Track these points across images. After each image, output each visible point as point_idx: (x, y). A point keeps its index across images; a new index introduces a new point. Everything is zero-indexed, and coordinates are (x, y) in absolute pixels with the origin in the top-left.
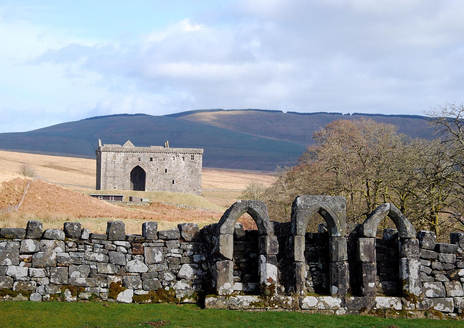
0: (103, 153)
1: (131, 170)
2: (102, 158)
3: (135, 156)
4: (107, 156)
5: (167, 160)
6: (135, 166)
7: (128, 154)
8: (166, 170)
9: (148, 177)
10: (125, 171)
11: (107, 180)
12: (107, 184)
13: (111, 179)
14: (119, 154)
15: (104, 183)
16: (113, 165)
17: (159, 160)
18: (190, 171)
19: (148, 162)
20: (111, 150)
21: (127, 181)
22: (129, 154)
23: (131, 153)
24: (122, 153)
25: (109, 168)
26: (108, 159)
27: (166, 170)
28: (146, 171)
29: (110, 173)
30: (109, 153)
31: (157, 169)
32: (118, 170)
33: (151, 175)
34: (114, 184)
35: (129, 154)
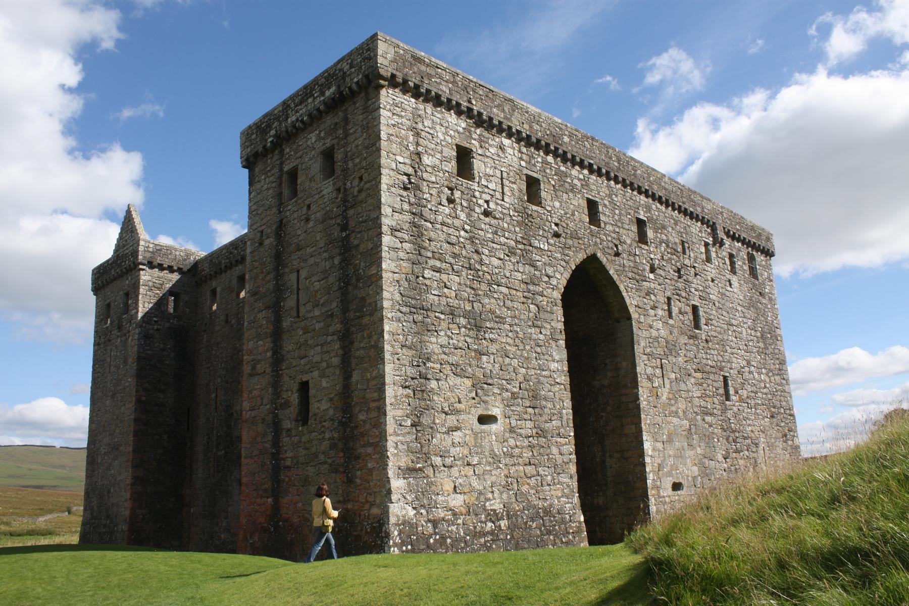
0: (388, 97)
1: (561, 278)
2: (383, 135)
3: (573, 189)
4: (417, 134)
5: (692, 255)
6: (581, 257)
7: (539, 156)
8: (695, 309)
9: (643, 344)
10: (534, 284)
11: (434, 344)
12: (433, 384)
13: (461, 336)
14: (496, 141)
15: (411, 371)
16: (463, 216)
17: (668, 246)
18: (759, 334)
19: (630, 246)
20: (445, 90)
21: (554, 366)
22: (545, 162)
23: (550, 158)
24: (506, 142)
25: (437, 238)
26: (427, 160)
27: (695, 309)
28: (631, 300)
29: (444, 277)
30: (429, 108)
31: (669, 299)
32: (496, 262)
33: (654, 333)
34: (480, 386)
35: (545, 162)
